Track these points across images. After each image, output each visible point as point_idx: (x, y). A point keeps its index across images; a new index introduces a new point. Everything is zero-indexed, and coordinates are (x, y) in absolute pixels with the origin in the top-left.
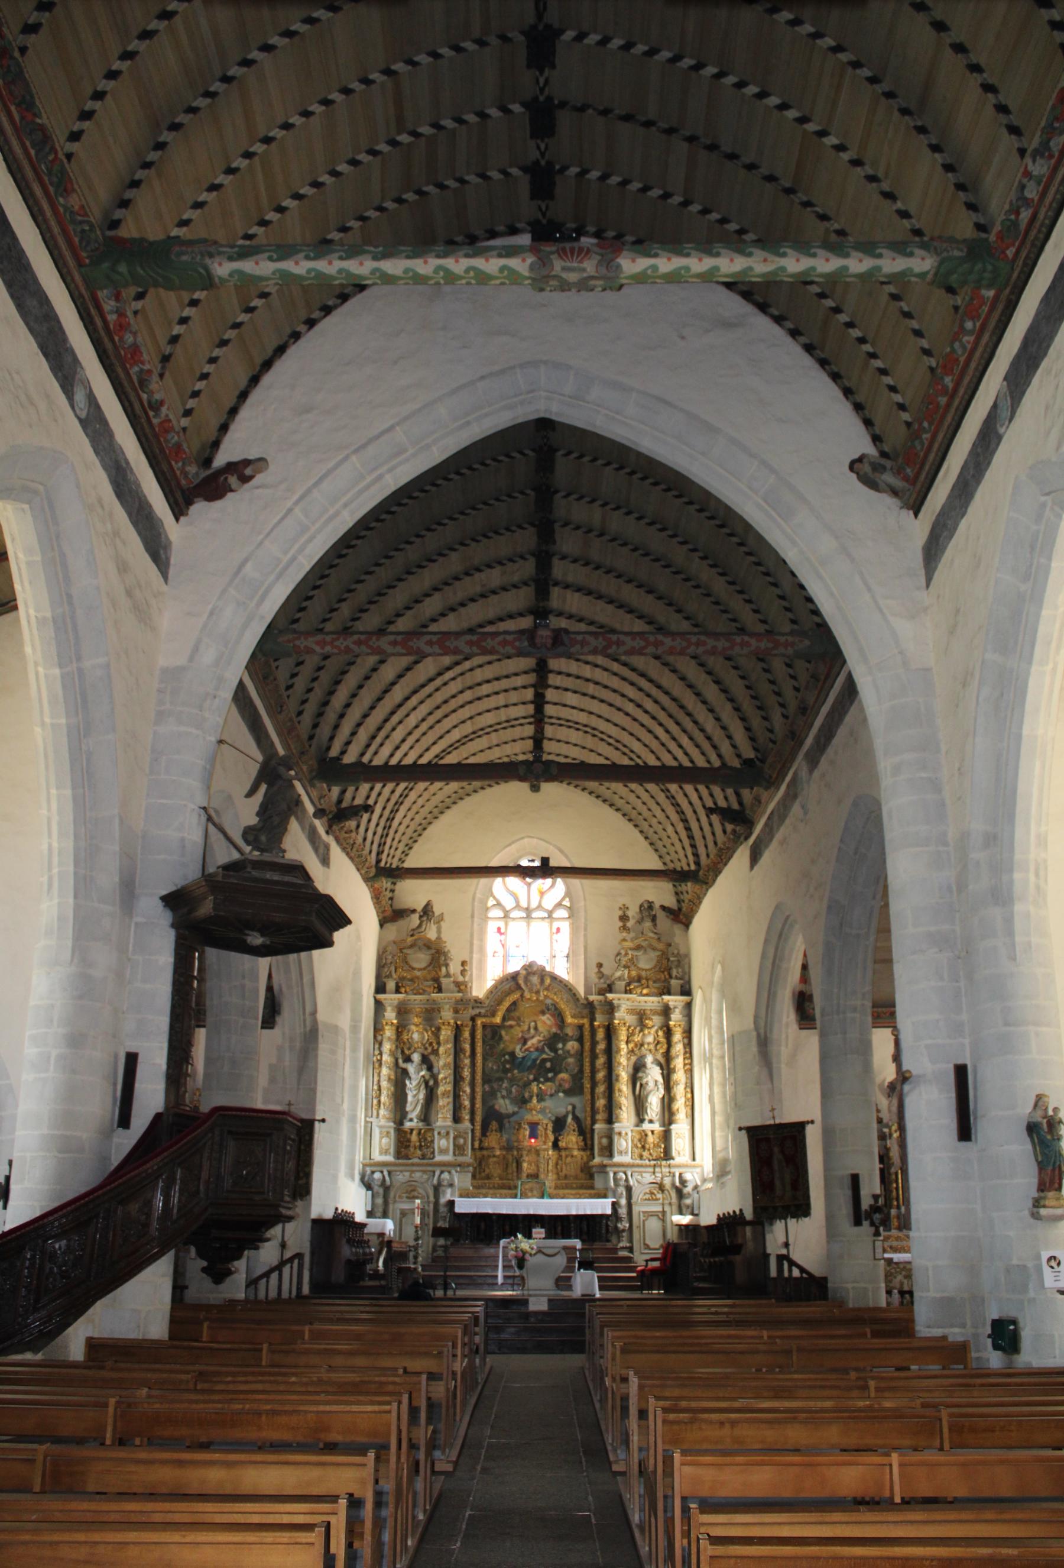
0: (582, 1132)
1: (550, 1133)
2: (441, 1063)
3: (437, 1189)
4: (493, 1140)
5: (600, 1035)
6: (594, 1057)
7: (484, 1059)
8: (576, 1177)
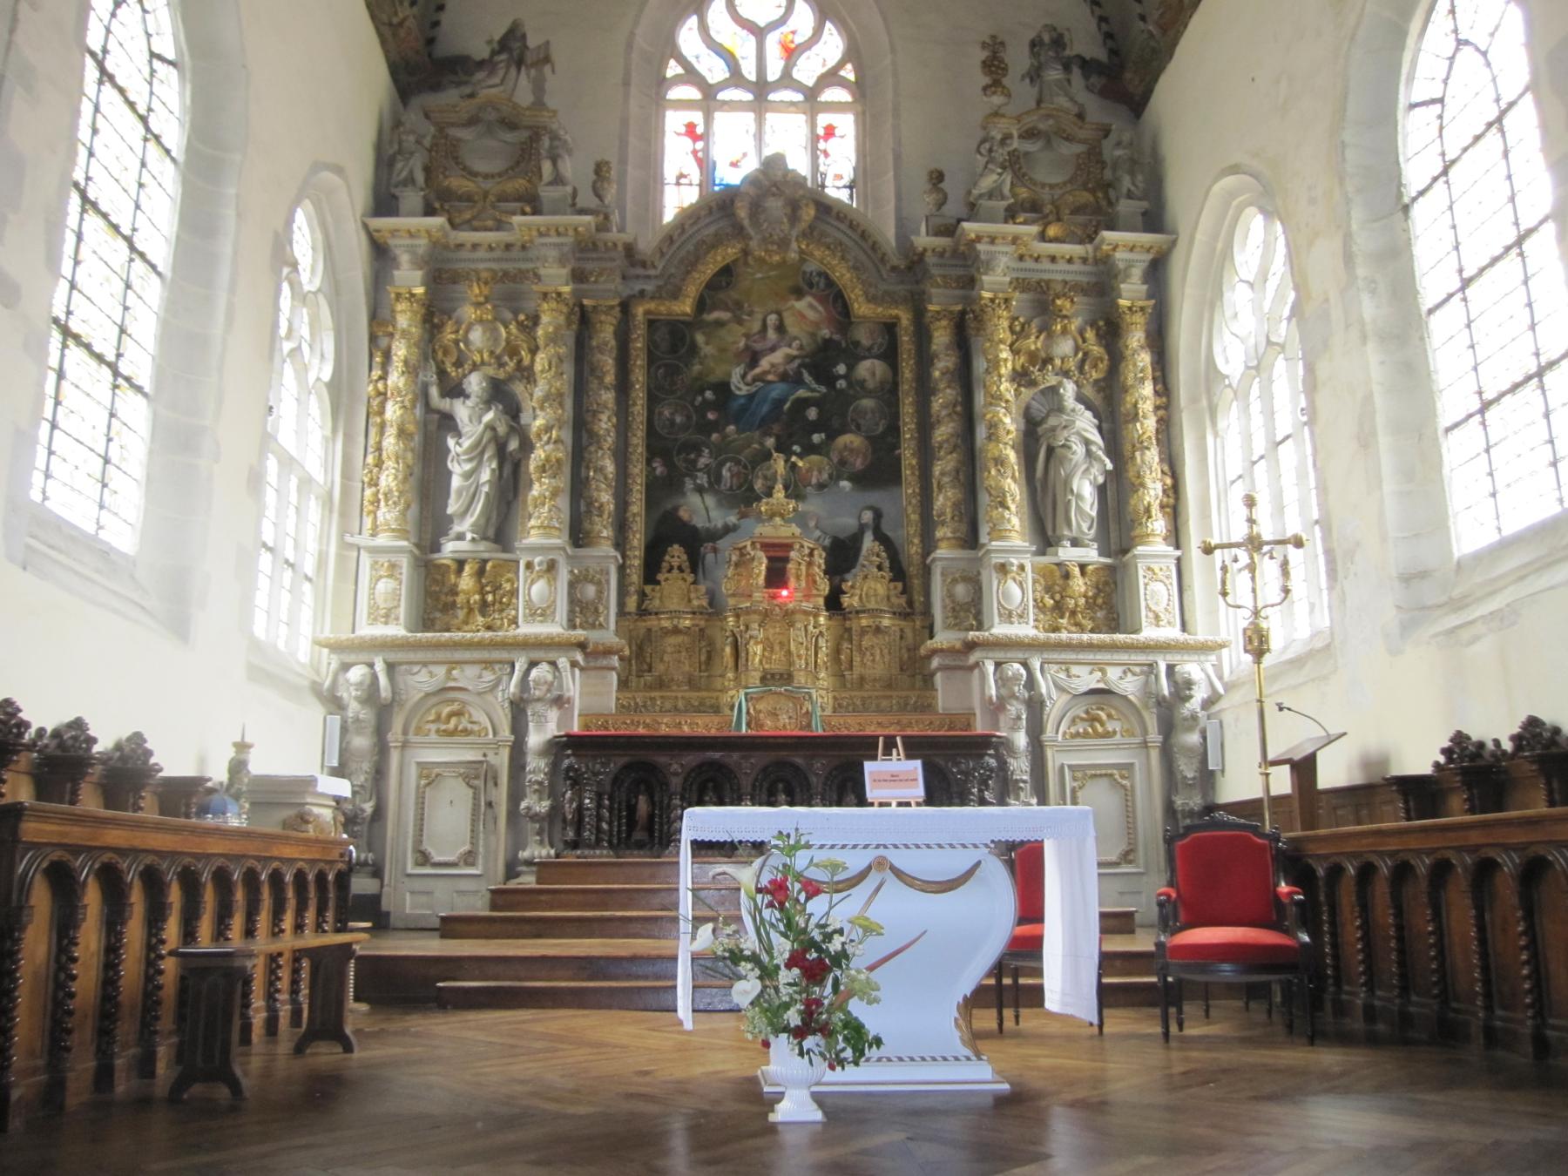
0: (898, 572)
1: (818, 572)
2: (539, 392)
3: (519, 711)
4: (674, 591)
5: (941, 337)
6: (925, 389)
7: (653, 400)
8: (889, 685)
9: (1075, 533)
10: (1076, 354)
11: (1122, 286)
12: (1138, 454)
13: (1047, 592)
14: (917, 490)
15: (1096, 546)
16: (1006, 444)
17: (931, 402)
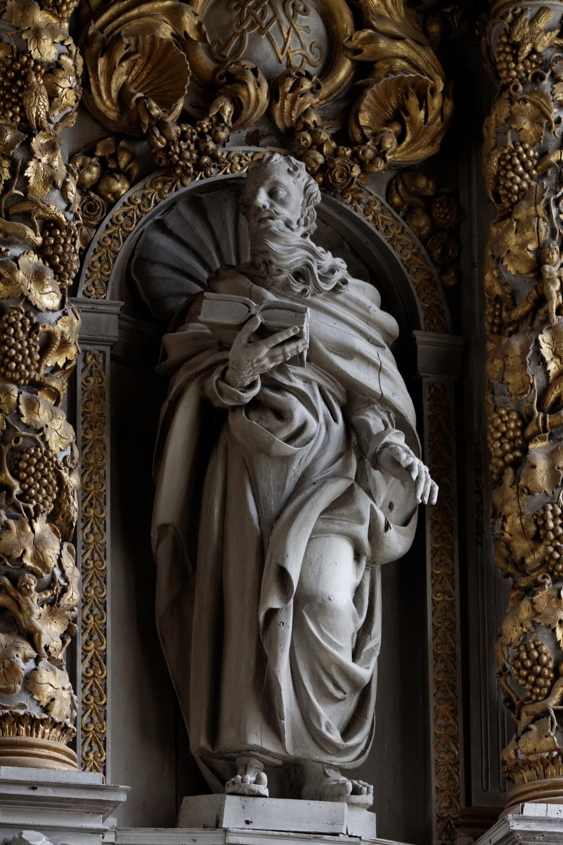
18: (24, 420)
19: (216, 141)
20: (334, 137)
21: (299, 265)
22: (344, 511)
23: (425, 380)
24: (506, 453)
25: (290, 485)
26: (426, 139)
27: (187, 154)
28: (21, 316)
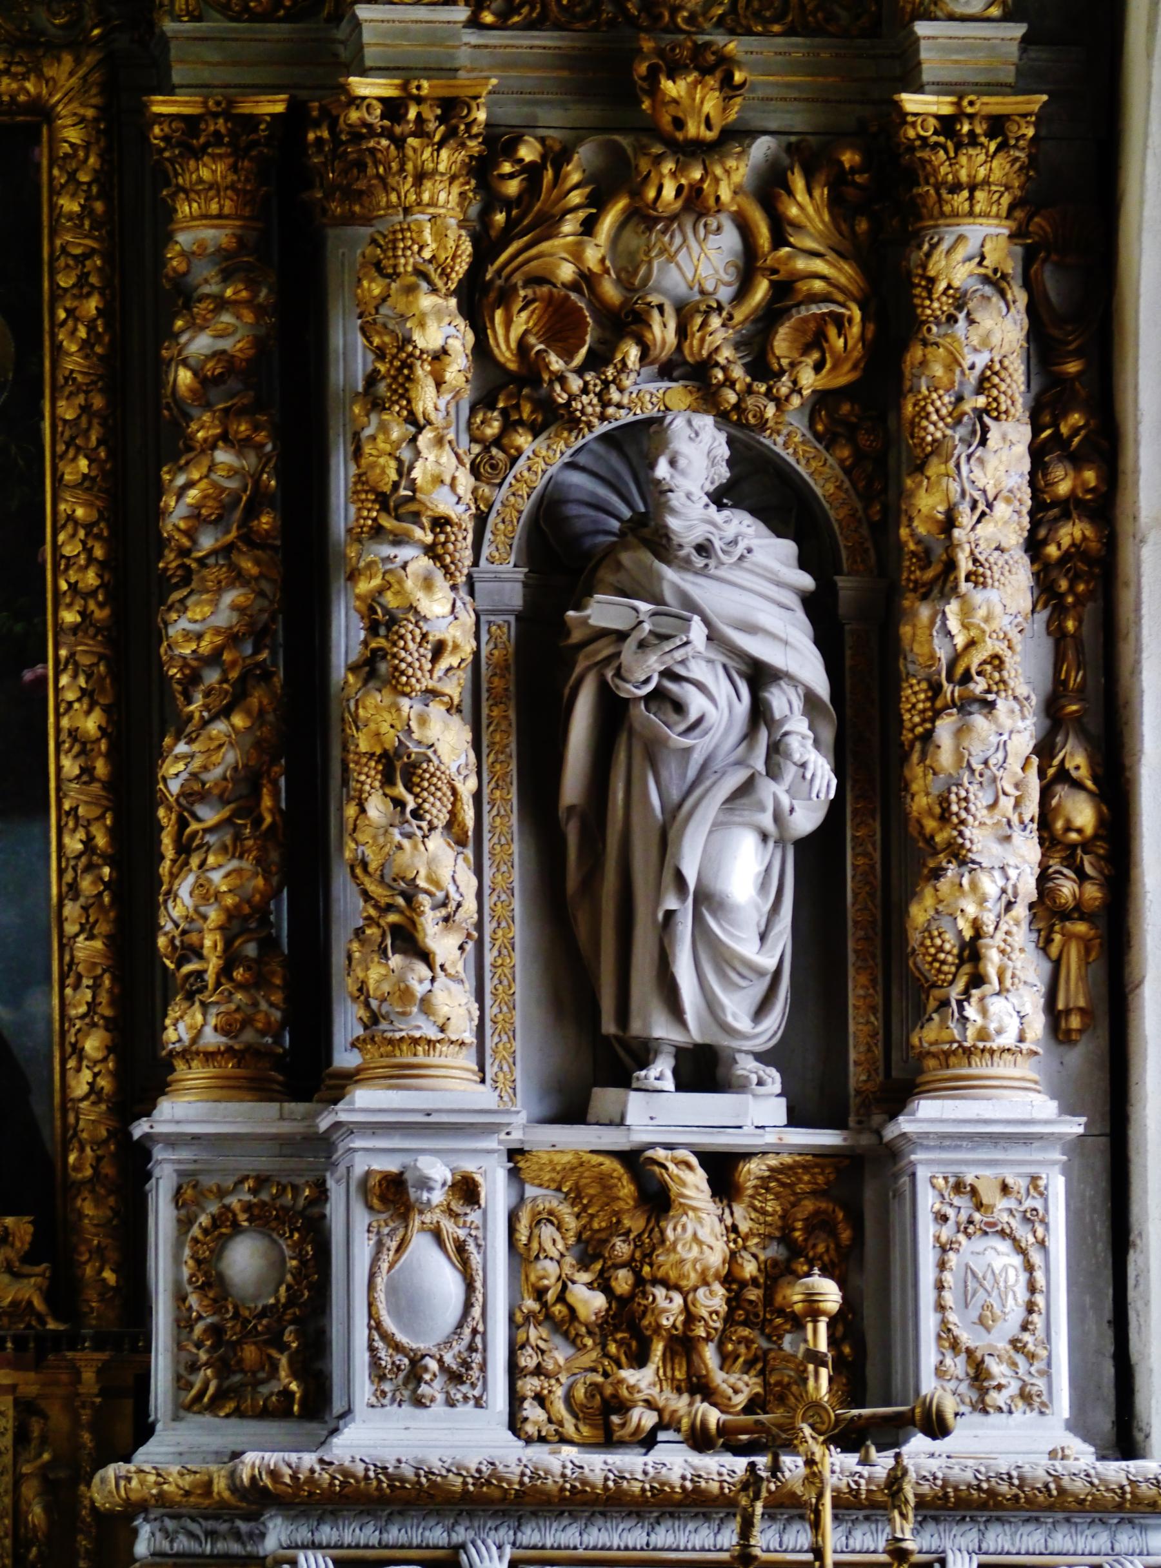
9: (696, 1031)
10: (742, 294)
11: (922, 28)
12: (945, 729)
13: (584, 1264)
14: (101, 841)
15: (774, 1079)
16: (433, 693)
17: (160, 490)
18: (415, 736)
19: (621, 390)
20: (749, 369)
21: (700, 540)
22: (745, 801)
23: (847, 627)
24: (915, 726)
25: (692, 773)
26: (847, 367)
27: (589, 410)
28: (411, 627)
